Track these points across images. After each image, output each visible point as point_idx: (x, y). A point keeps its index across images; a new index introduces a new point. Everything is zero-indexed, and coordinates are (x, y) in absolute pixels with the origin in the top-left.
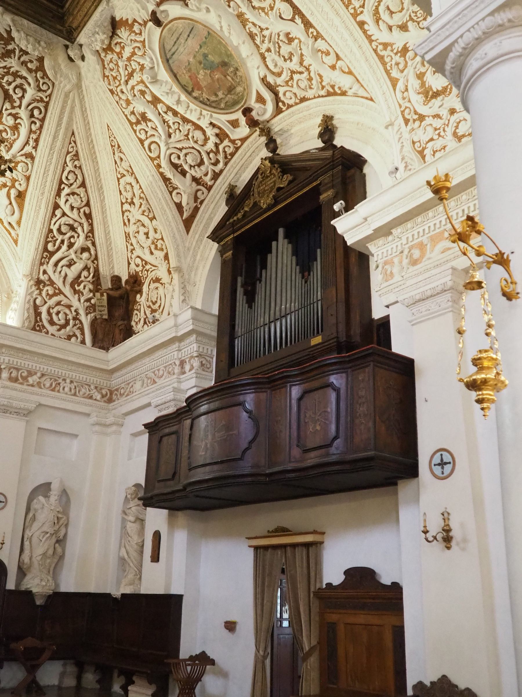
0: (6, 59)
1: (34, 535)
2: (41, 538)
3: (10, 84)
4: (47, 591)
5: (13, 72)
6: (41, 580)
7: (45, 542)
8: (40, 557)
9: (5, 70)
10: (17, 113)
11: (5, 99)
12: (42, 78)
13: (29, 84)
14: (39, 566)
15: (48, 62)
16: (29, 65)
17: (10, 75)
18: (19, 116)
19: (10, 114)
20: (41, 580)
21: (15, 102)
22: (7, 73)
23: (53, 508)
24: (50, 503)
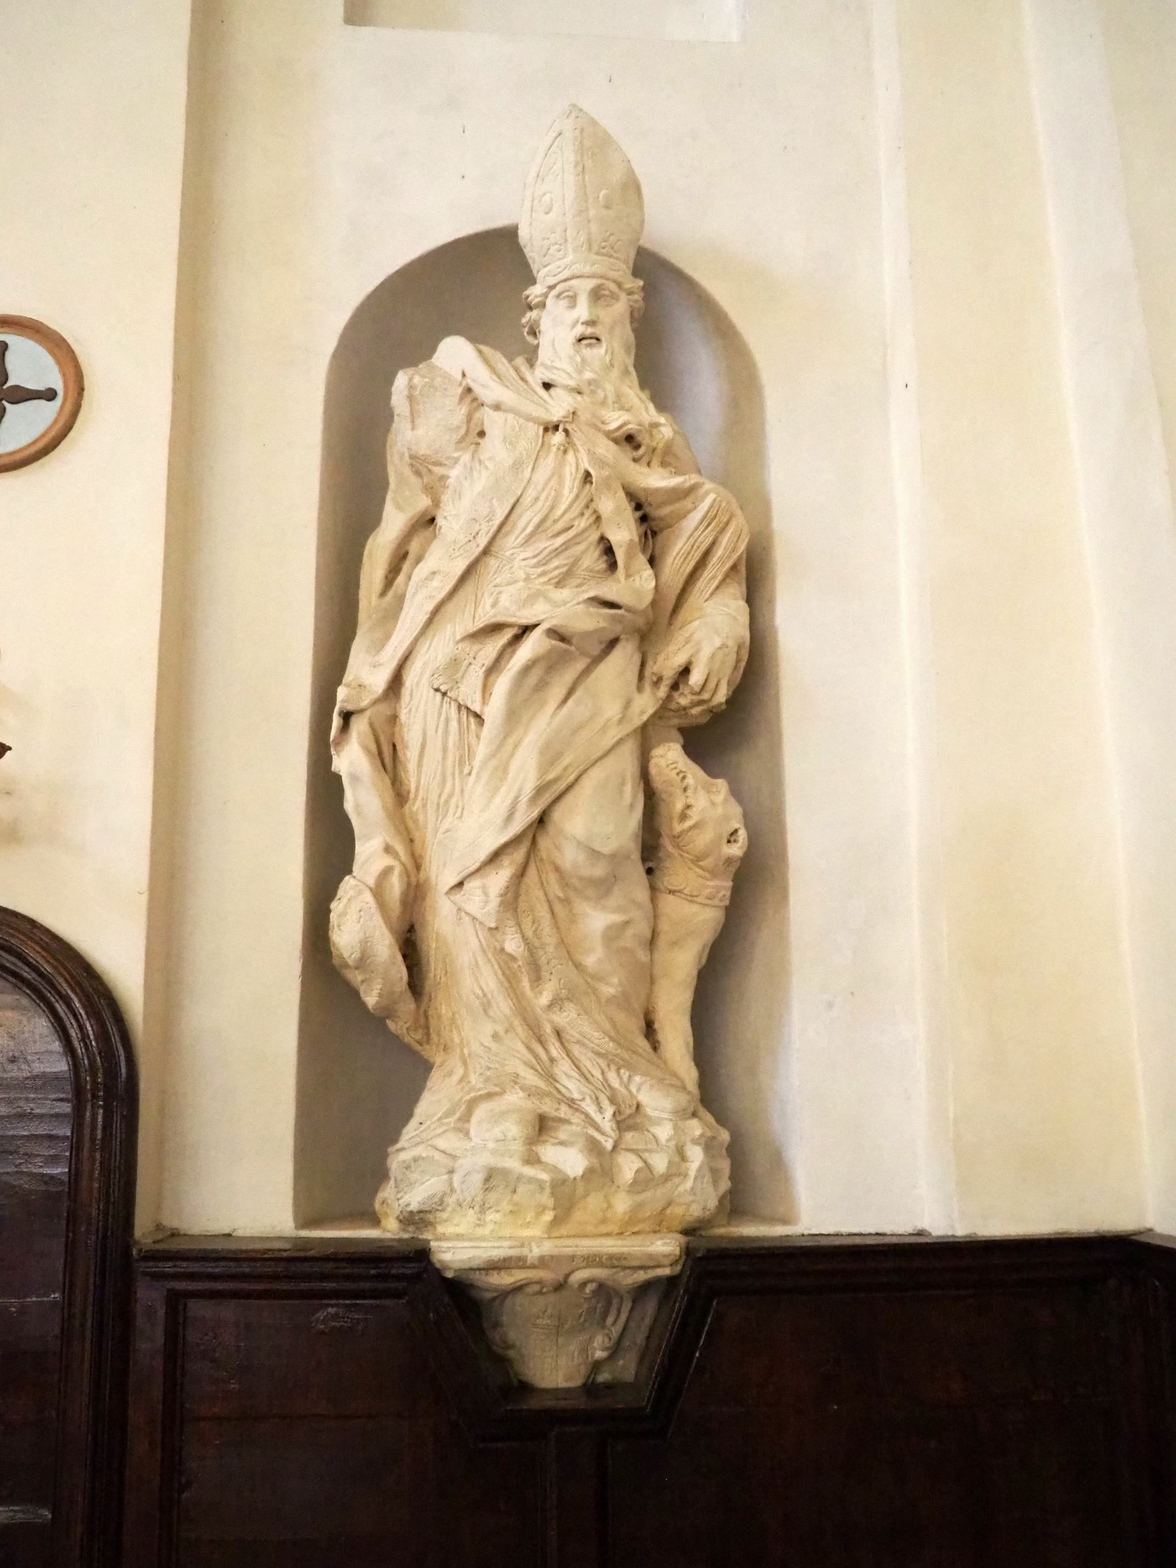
1: (410, 678)
2: (469, 691)
4: (610, 1246)
6: (542, 1126)
7: (513, 716)
8: (500, 878)
14: (510, 981)
20: (542, 1126)
23: (558, 406)
24: (540, 374)
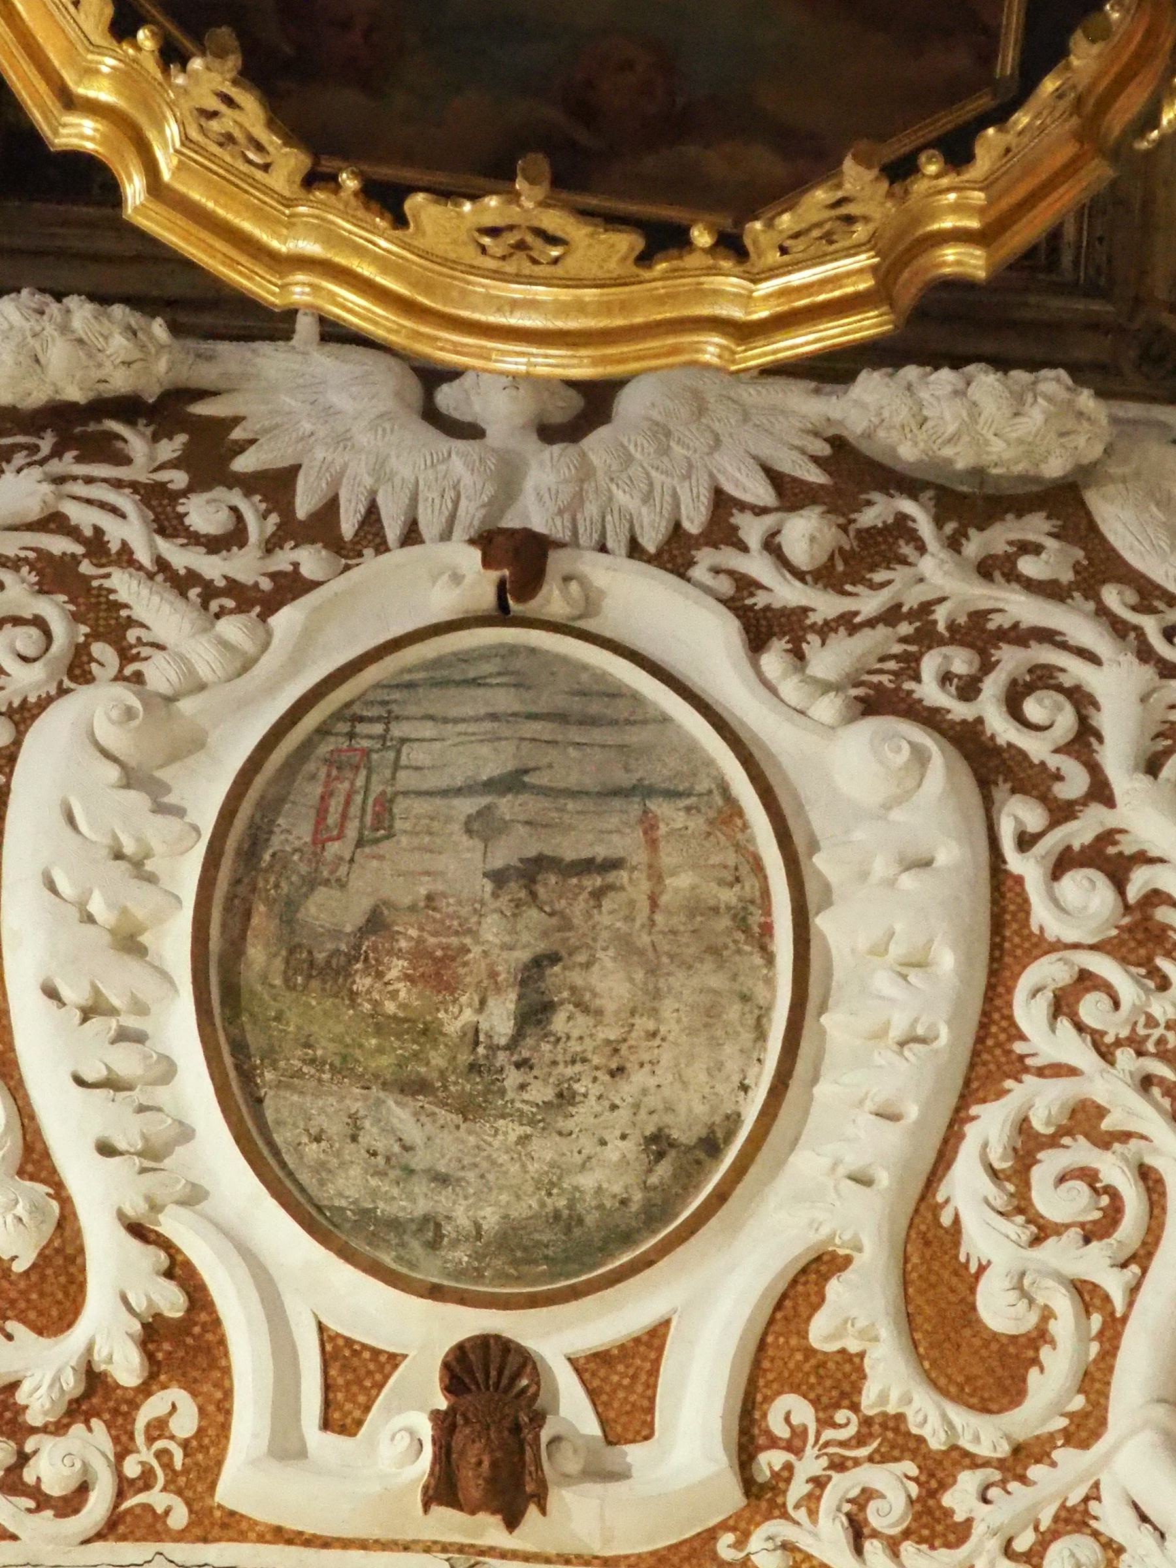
0: (879, 576)
3: (969, 690)
5: (952, 627)
9: (905, 629)
10: (1108, 836)
11: (985, 785)
12: (1144, 607)
13: (1092, 658)
15: (1128, 515)
16: (1028, 566)
17: (942, 642)
18: (1128, 849)
19: (1063, 863)
21: (1058, 777)
22: (927, 637)
